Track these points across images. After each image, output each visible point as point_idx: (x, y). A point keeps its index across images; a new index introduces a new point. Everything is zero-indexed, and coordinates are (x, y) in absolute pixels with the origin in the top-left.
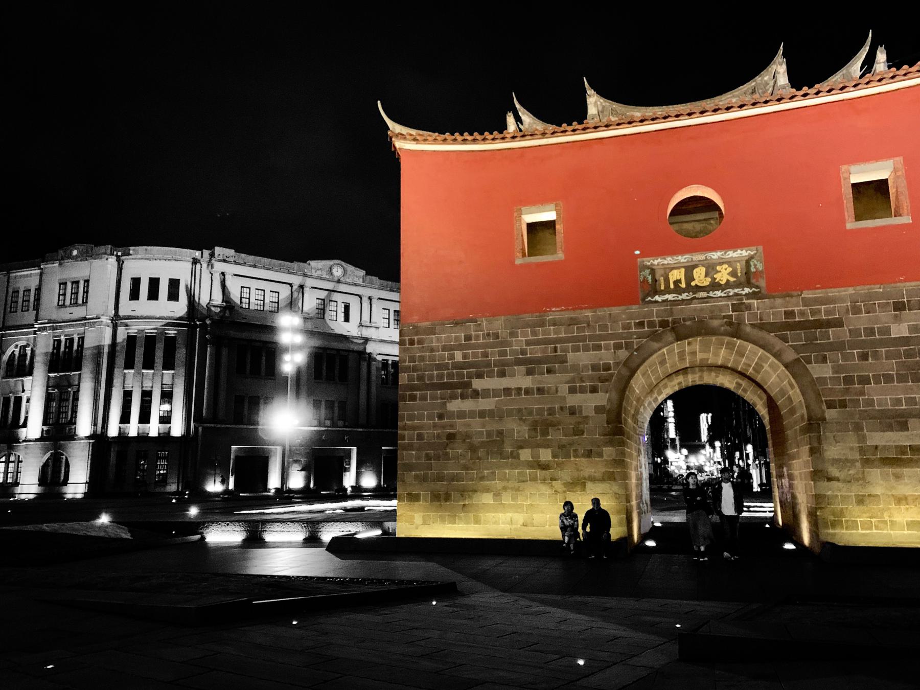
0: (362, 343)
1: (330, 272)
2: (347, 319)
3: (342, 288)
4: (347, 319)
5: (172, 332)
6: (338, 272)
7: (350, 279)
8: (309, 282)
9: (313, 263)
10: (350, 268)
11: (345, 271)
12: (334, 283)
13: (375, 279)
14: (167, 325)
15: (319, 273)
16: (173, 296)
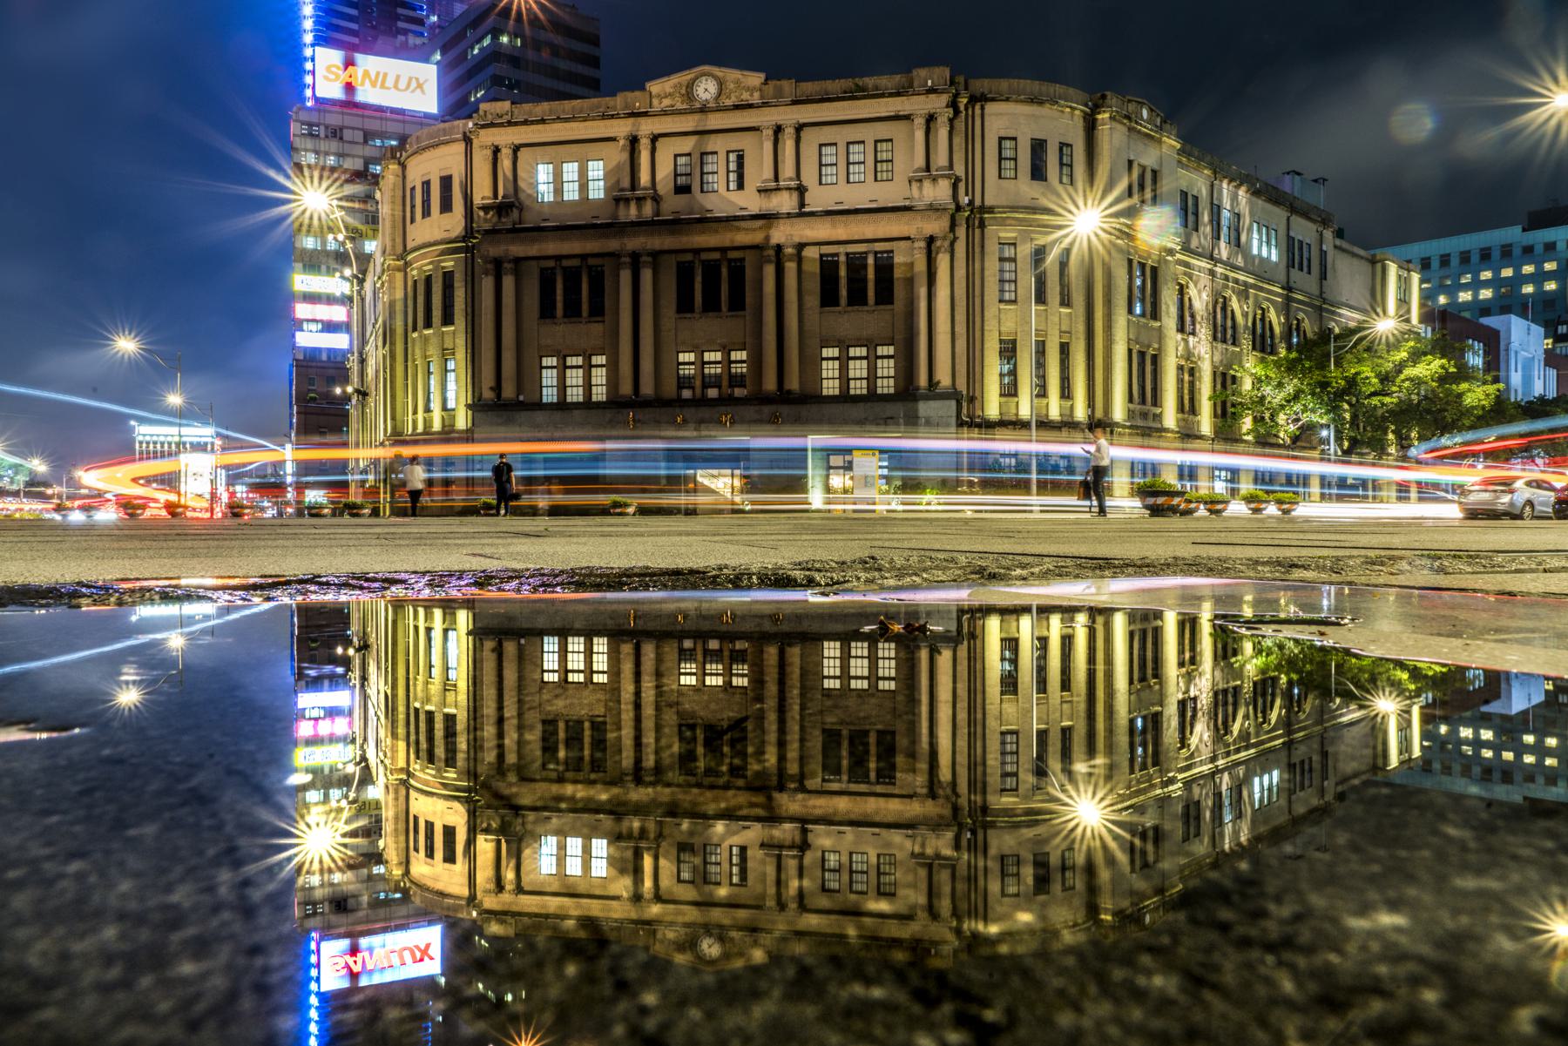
0: (760, 228)
1: (689, 94)
2: (741, 186)
3: (715, 121)
4: (741, 186)
5: (449, 264)
6: (706, 90)
7: (733, 99)
8: (647, 127)
9: (655, 87)
10: (732, 75)
11: (721, 84)
12: (697, 117)
13: (787, 86)
14: (443, 253)
15: (666, 102)
16: (446, 206)
